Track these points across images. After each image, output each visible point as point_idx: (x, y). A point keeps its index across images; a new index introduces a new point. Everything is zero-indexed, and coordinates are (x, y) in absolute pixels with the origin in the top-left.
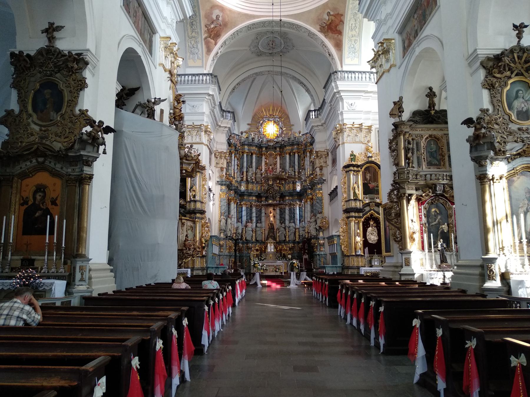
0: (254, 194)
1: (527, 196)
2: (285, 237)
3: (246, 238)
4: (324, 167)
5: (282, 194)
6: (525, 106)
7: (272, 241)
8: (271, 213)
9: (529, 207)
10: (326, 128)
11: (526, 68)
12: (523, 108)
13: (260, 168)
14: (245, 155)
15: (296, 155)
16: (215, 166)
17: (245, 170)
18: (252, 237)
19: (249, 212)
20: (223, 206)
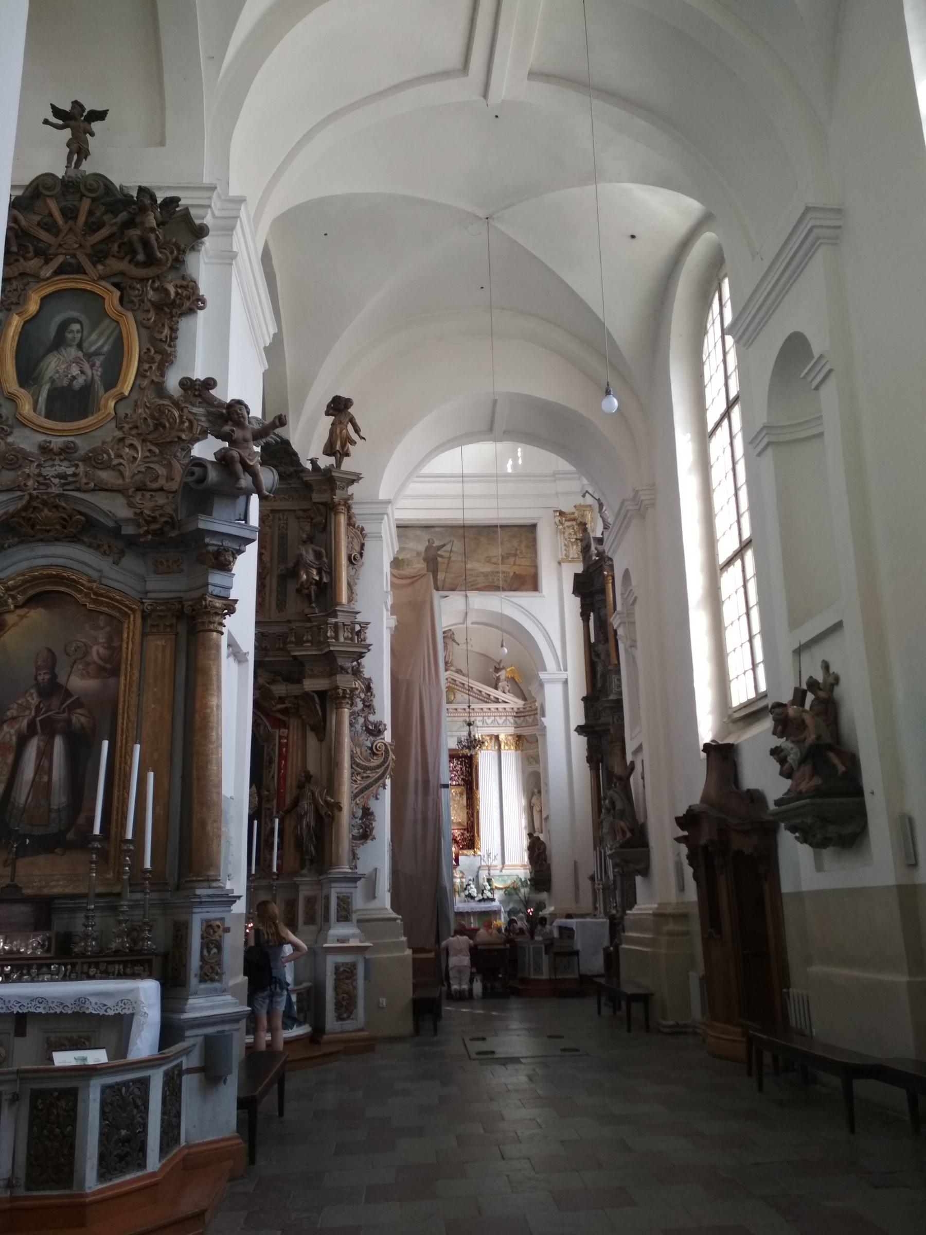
1: (40, 678)
6: (82, 372)
9: (38, 719)
11: (92, 246)
12: (74, 378)
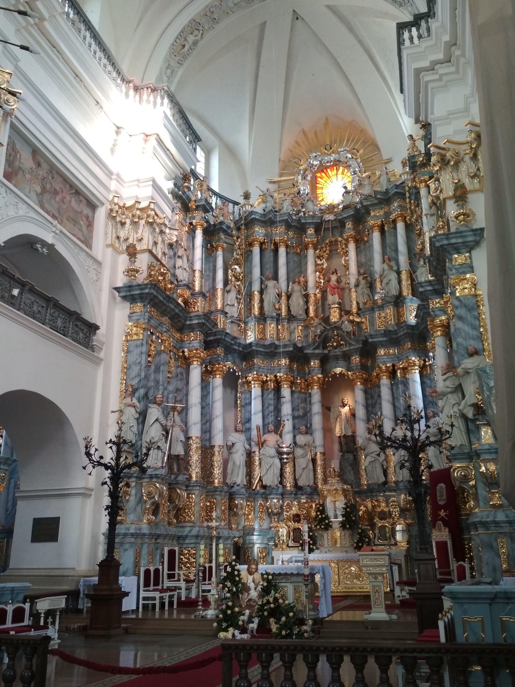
0: (281, 350)
2: (385, 472)
3: (260, 480)
4: (475, 191)
5: (365, 342)
7: (339, 486)
8: (344, 406)
10: (462, 60)
13: (302, 279)
14: (256, 250)
15: (400, 226)
16: (108, 246)
17: (256, 287)
18: (282, 475)
19: (272, 402)
20: (133, 367)
